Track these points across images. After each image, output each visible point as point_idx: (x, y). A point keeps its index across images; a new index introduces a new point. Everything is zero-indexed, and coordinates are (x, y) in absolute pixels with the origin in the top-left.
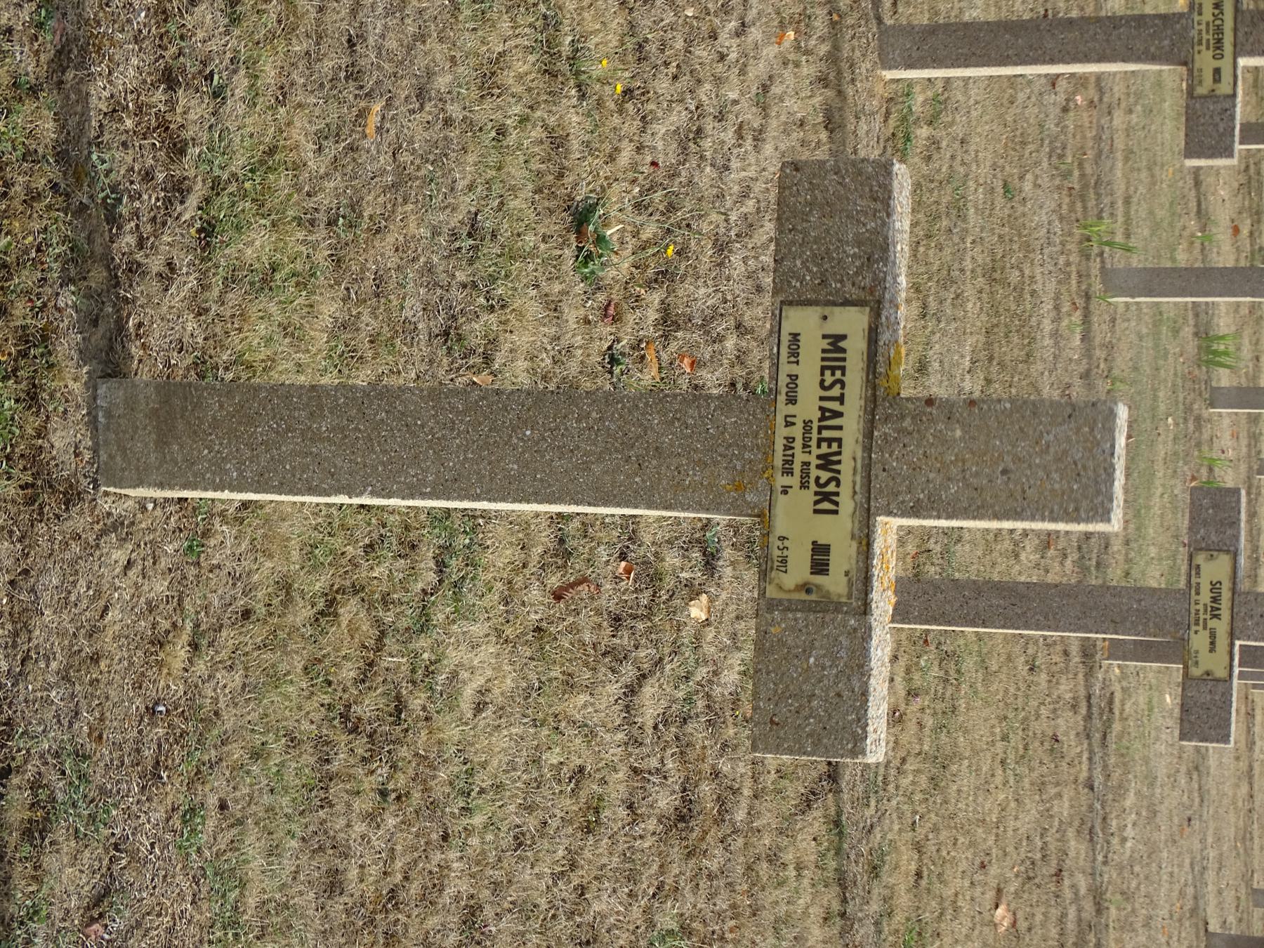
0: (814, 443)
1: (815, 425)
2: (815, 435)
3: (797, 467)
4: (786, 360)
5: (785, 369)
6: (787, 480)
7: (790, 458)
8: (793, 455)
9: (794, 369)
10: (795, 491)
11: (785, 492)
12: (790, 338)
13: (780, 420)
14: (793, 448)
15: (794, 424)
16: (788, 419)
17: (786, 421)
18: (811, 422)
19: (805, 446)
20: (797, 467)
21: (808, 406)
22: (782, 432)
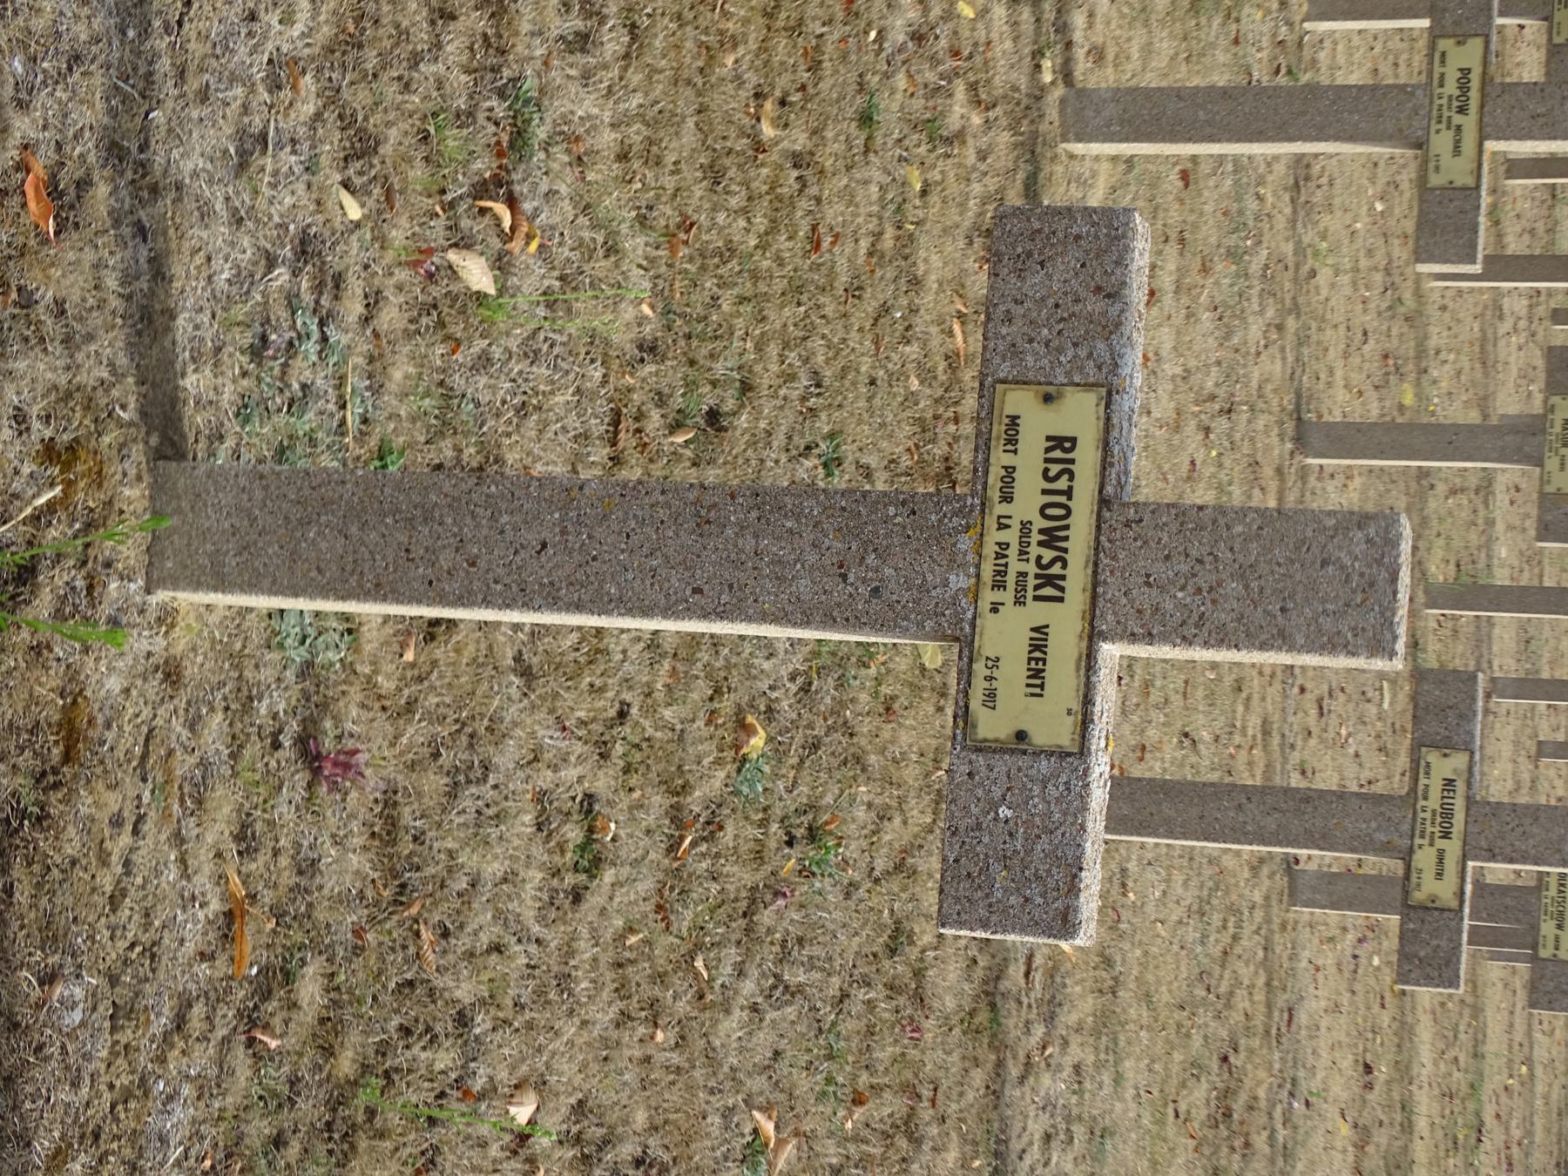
0: (1034, 550)
4: (1002, 448)
6: (998, 596)
8: (1006, 565)
9: (1008, 460)
10: (1009, 609)
11: (995, 610)
12: (1007, 421)
15: (1008, 527)
19: (1022, 553)
20: (1011, 579)
21: (1028, 502)
22: (994, 536)
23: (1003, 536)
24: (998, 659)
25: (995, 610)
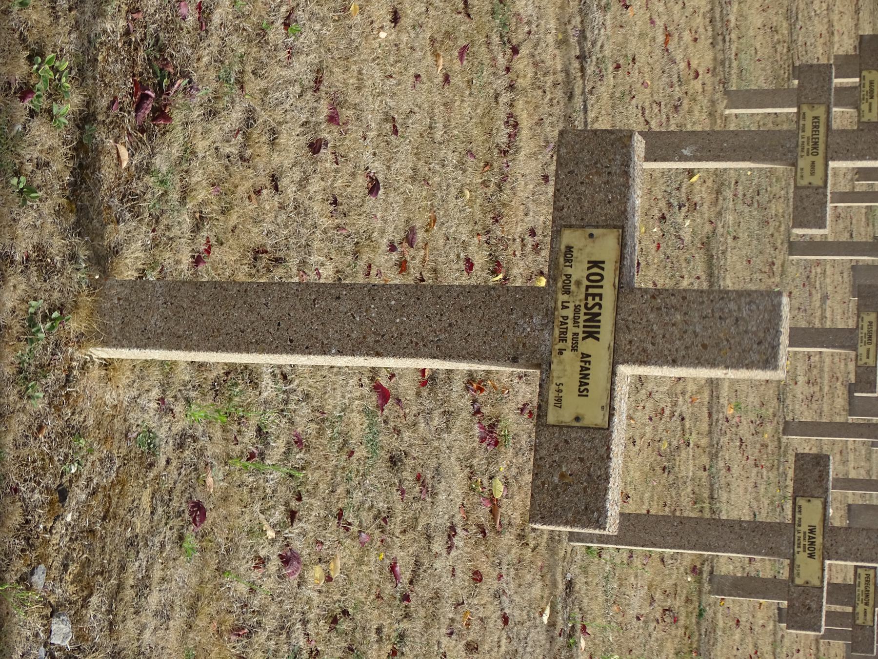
0: (581, 321)
8: (567, 328)
15: (568, 307)
20: (569, 336)
23: (565, 313)
25: (561, 352)
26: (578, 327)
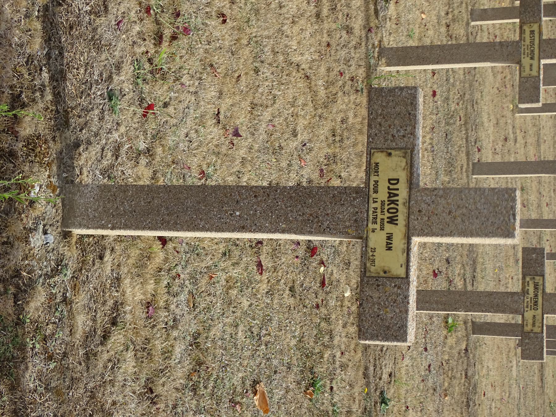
0: (386, 210)
1: (387, 203)
2: (386, 207)
3: (379, 221)
4: (373, 175)
5: (373, 178)
6: (375, 226)
7: (376, 217)
8: (377, 215)
9: (376, 178)
11: (373, 231)
12: (374, 165)
13: (372, 202)
14: (377, 212)
15: (377, 202)
16: (374, 200)
17: (374, 201)
18: (384, 201)
19: (382, 212)
20: (379, 221)
21: (383, 195)
23: (375, 205)
24: (375, 248)
25: (373, 231)
26: (384, 214)
